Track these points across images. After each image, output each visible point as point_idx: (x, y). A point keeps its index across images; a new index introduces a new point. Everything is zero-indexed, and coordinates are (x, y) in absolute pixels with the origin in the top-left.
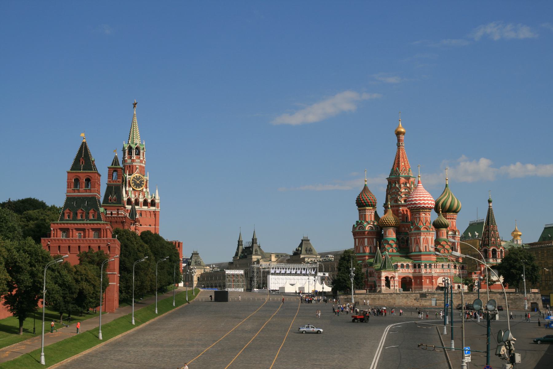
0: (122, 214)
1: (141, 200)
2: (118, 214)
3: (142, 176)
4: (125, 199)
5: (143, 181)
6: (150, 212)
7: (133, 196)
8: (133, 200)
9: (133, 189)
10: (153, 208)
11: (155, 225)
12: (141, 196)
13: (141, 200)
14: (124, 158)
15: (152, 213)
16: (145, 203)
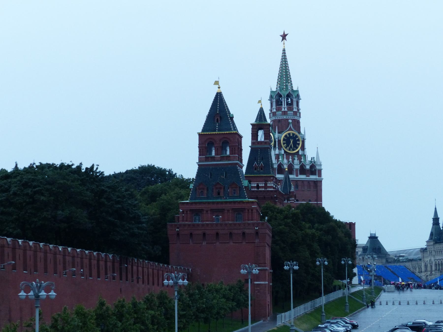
0: (271, 187)
1: (297, 166)
2: (266, 187)
3: (297, 133)
4: (275, 166)
5: (299, 140)
6: (309, 182)
8: (286, 167)
9: (285, 152)
10: (312, 177)
11: (317, 200)
12: (296, 161)
13: (297, 166)
14: (271, 111)
15: (312, 184)
16: (303, 170)
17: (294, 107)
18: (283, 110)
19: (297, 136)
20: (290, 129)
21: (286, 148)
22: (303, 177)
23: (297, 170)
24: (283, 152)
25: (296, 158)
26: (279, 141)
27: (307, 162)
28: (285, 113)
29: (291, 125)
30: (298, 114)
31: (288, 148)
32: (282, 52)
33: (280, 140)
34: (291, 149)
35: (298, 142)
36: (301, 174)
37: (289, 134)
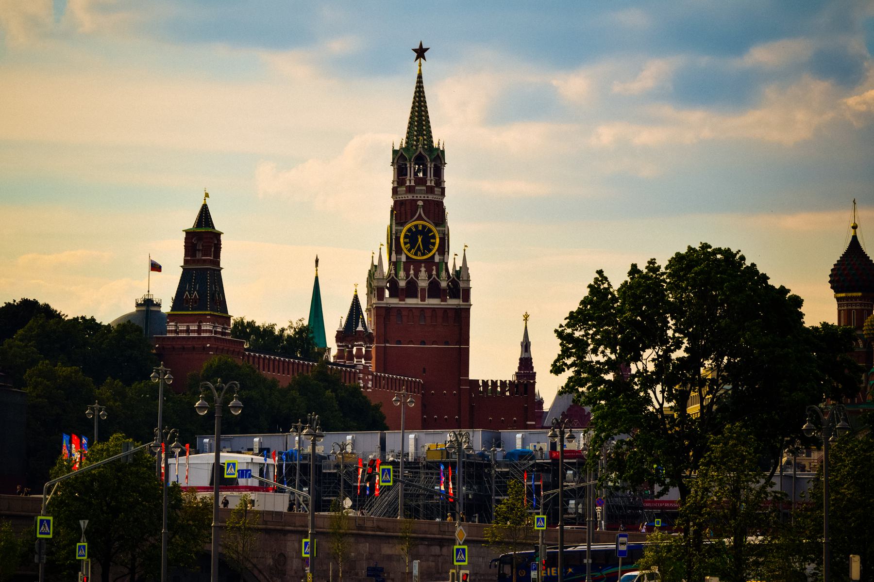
5: (434, 237)
7: (402, 274)
8: (402, 284)
9: (407, 257)
10: (452, 302)
12: (423, 274)
16: (434, 290)
17: (429, 178)
18: (408, 184)
19: (430, 230)
20: (420, 218)
21: (409, 251)
22: (434, 302)
23: (423, 290)
24: (404, 258)
25: (423, 269)
26: (398, 239)
27: (443, 274)
28: (410, 190)
29: (420, 211)
30: (437, 190)
31: (413, 251)
32: (415, 80)
33: (399, 237)
34: (419, 253)
35: (432, 241)
36: (431, 296)
37: (416, 226)
